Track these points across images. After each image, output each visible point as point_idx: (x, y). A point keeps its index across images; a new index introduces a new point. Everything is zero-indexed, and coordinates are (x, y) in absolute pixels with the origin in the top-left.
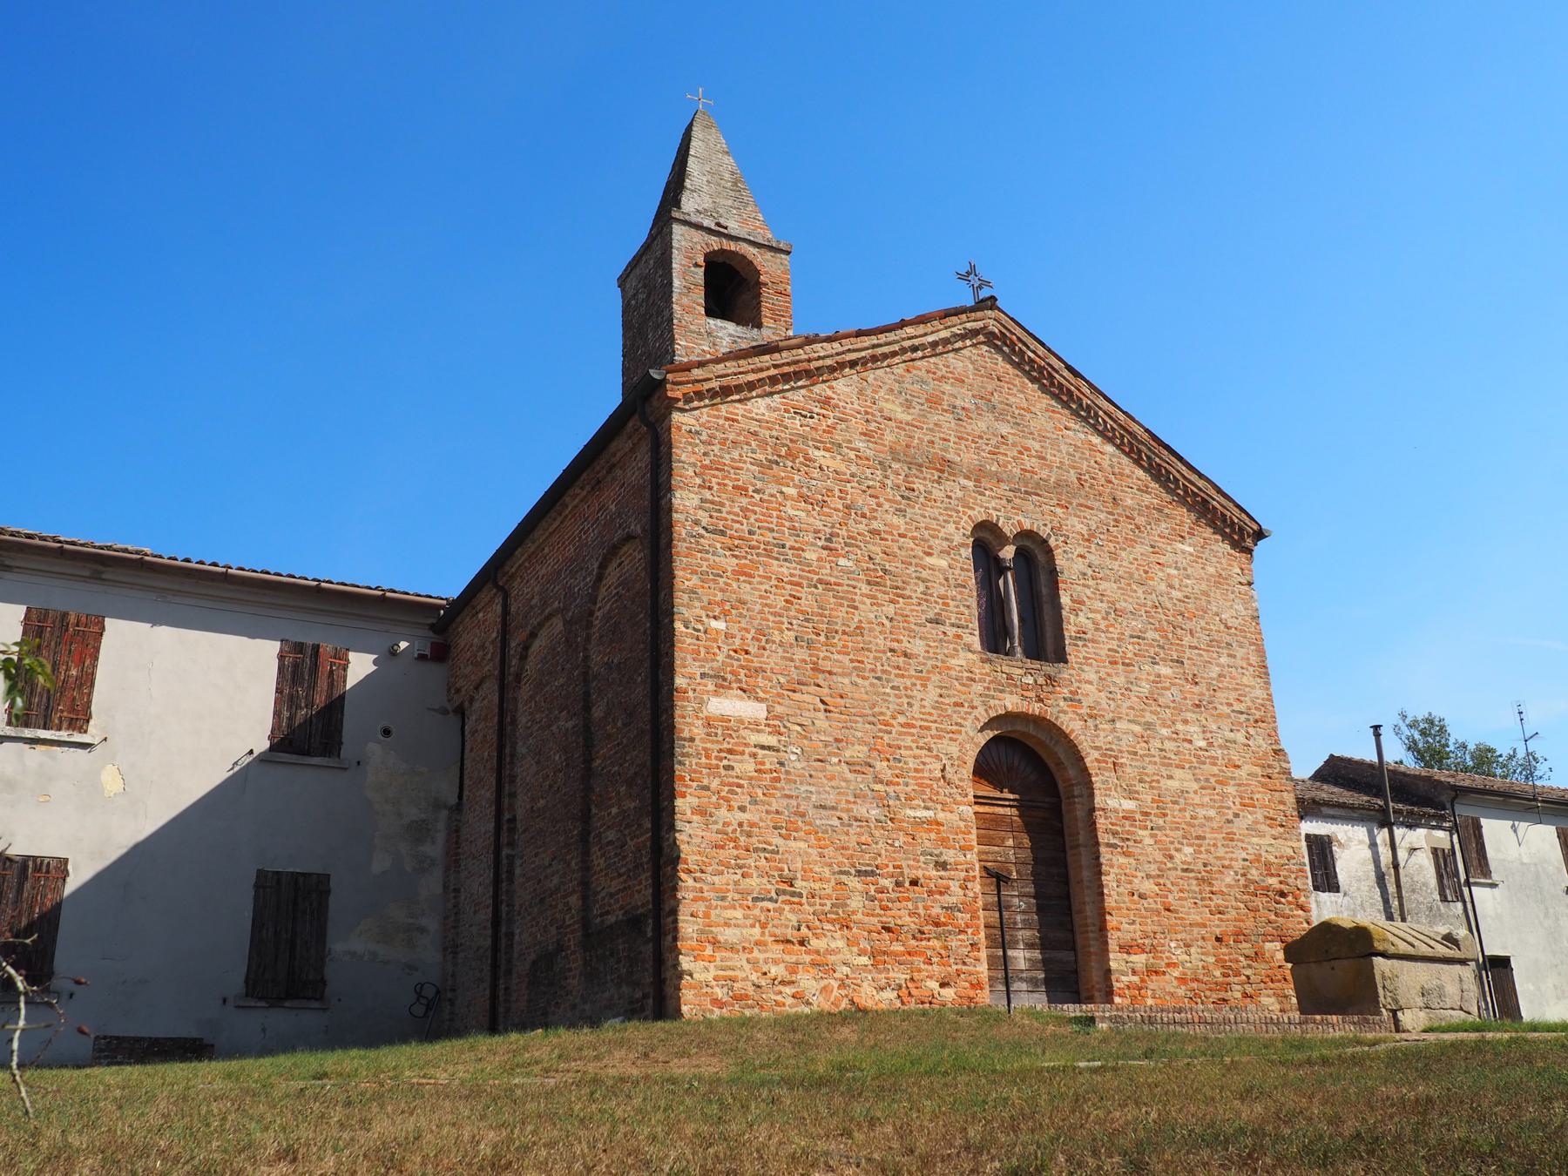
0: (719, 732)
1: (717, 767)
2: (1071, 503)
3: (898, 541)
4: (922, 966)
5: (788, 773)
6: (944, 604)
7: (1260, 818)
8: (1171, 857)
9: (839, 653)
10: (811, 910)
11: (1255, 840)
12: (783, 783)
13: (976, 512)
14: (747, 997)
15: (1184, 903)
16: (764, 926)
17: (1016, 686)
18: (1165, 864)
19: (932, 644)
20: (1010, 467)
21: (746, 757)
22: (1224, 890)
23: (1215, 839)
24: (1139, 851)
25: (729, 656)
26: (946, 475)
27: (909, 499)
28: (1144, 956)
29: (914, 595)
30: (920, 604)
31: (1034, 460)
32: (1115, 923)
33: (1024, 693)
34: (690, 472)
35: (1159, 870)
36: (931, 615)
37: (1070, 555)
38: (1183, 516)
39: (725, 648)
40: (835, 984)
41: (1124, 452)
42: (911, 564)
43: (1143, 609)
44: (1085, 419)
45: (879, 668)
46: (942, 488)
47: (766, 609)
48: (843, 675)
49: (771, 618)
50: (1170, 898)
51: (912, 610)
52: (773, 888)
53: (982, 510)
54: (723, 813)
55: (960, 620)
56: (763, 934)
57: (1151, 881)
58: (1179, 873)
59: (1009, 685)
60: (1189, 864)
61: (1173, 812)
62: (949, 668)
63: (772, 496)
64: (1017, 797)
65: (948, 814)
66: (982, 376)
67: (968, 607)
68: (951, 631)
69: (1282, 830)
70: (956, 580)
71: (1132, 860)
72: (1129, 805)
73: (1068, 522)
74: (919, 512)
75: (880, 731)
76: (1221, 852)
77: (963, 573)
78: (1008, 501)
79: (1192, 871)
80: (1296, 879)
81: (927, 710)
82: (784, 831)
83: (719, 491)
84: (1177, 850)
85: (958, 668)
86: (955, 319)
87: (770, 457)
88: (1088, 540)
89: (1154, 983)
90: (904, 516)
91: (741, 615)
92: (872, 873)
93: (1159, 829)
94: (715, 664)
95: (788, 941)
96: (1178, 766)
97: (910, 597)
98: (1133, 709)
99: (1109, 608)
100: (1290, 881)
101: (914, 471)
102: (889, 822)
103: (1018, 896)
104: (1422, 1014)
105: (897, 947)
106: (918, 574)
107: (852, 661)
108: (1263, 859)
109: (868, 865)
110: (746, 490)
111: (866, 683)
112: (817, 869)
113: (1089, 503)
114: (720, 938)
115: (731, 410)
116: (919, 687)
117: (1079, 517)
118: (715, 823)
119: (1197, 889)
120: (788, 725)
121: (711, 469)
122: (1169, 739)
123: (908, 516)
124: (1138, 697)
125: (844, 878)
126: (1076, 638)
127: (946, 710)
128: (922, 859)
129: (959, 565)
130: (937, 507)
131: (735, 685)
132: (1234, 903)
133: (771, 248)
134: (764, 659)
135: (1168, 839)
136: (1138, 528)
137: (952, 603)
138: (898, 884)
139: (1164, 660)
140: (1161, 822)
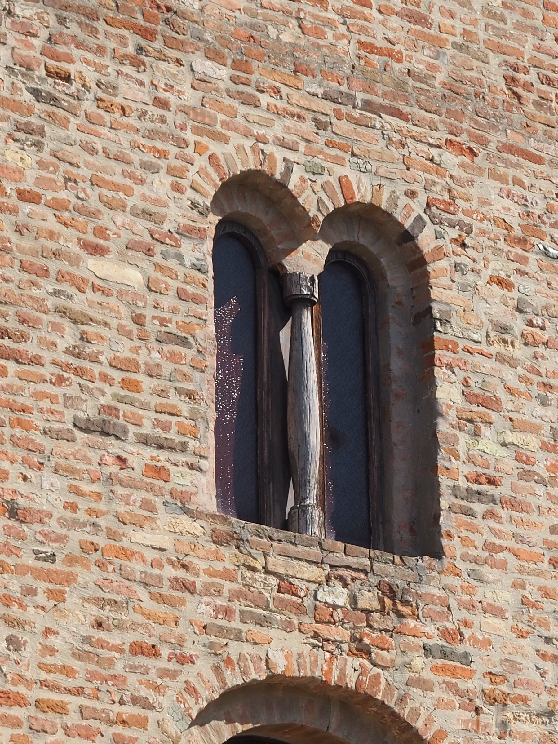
2: (483, 143)
3: (14, 211)
6: (126, 384)
13: (230, 149)
17: (300, 609)
19: (86, 487)
20: (330, 35)
26: (158, 44)
27: (53, 100)
29: (47, 356)
30: (60, 380)
31: (394, 21)
33: (323, 629)
37: (471, 278)
42: (45, 273)
46: (145, 78)
51: (40, 396)
53: (248, 143)
55: (166, 427)
59: (283, 606)
62: (127, 554)
67: (190, 395)
70: (163, 322)
73: (473, 191)
74: (78, 136)
77: (182, 306)
78: (320, 125)
81: (58, 660)
85: (150, 555)
88: (522, 242)
90: (38, 145)
97: (36, 361)
101: (74, 29)
106: (62, 302)
113: (532, 146)
116: (41, 599)
117: (502, 179)
123: (49, 146)
127: (111, 662)
129: (174, 284)
130: (129, 128)
137: (147, 383)
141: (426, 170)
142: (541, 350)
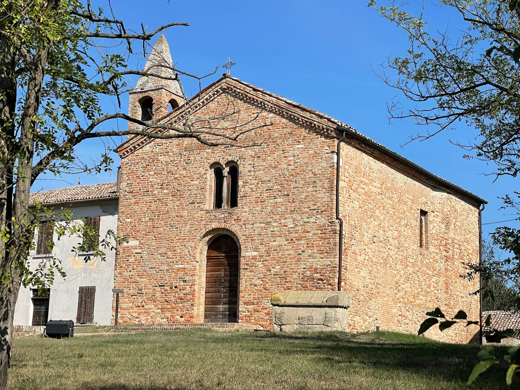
0: (126, 251)
1: (125, 261)
4: (175, 312)
5: (143, 259)
7: (315, 251)
8: (270, 270)
9: (161, 221)
10: (146, 297)
11: (310, 260)
12: (141, 263)
14: (127, 322)
15: (273, 286)
16: (133, 303)
17: (217, 219)
21: (133, 257)
22: (292, 280)
23: (292, 262)
25: (131, 229)
27: (188, 163)
29: (186, 196)
32: (243, 295)
34: (125, 176)
36: (191, 201)
38: (304, 132)
39: (130, 226)
40: (150, 318)
41: (277, 114)
42: (186, 186)
43: (274, 178)
44: (261, 107)
45: (172, 222)
47: (142, 212)
48: (161, 227)
49: (143, 215)
52: (136, 292)
54: (126, 273)
56: (133, 305)
57: (260, 280)
58: (272, 276)
59: (214, 219)
60: (277, 272)
61: (273, 254)
62: (194, 218)
63: (146, 176)
64: (225, 255)
65: (188, 265)
66: (221, 106)
68: (196, 205)
69: (326, 254)
71: (252, 273)
72: (255, 253)
73: (247, 153)
75: (170, 242)
76: (293, 266)
78: (224, 152)
79: (278, 275)
82: (140, 276)
83: (132, 180)
84: (273, 268)
85: (197, 217)
86: (210, 89)
87: (147, 164)
88: (254, 157)
89: (256, 315)
91: (135, 216)
92: (164, 286)
94: (127, 232)
95: (139, 307)
96: (278, 236)
97: (185, 197)
98: (262, 218)
99: (259, 181)
100: (326, 275)
101: (191, 153)
102: (170, 270)
103: (223, 288)
104: (296, 326)
105: (169, 307)
107: (164, 222)
108: (314, 267)
109: (163, 283)
110: (139, 176)
111: (168, 228)
112: (148, 286)
114: (122, 307)
115: (138, 152)
117: (252, 149)
118: (123, 276)
119: (279, 281)
120: (144, 245)
121: (130, 173)
122: (276, 227)
124: (265, 213)
125: (155, 288)
126: (244, 196)
128: (179, 280)
131: (131, 237)
132: (296, 285)
133: (157, 89)
134: (140, 227)
135: (269, 264)
136: (278, 145)
137: (198, 195)
138: (171, 288)
139: (280, 196)
140: (268, 258)
141: (239, 152)
142: (256, 172)
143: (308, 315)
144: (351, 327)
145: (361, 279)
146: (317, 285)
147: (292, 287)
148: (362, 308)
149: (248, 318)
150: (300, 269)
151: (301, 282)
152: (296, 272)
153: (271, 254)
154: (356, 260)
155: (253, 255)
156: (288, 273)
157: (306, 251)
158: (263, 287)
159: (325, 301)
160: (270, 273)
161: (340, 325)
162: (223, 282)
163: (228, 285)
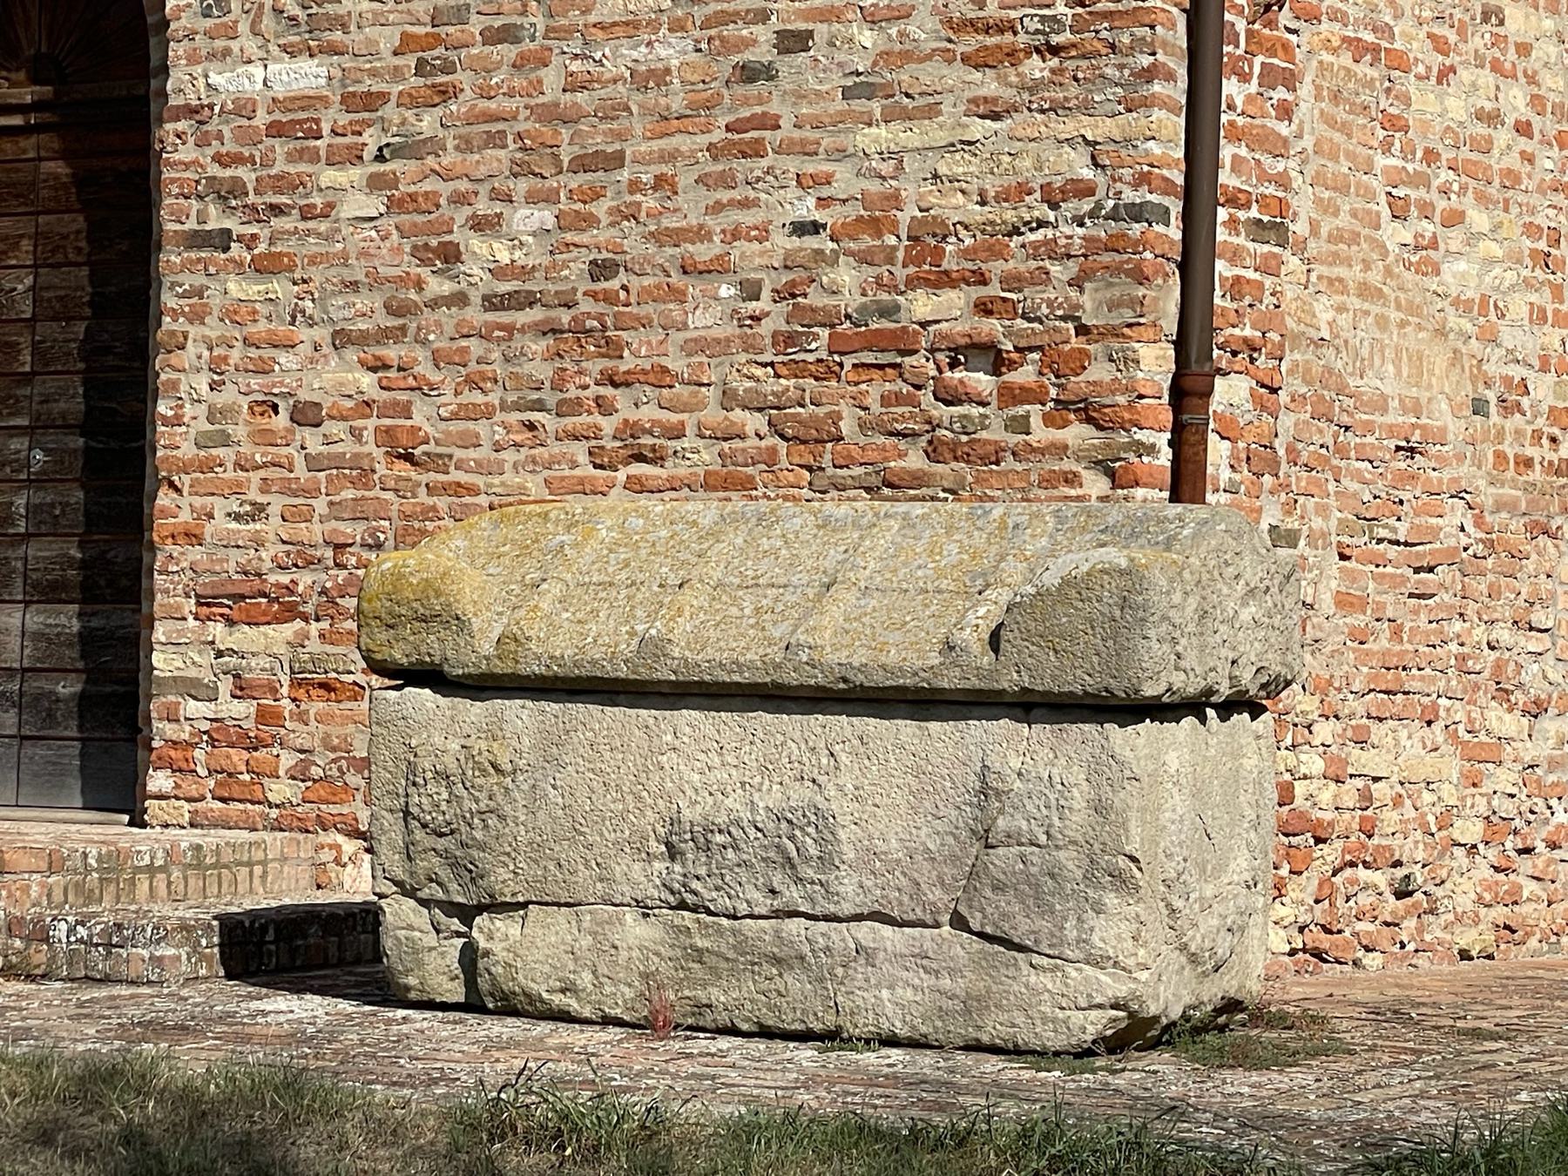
8: (450, 255)
15: (481, 427)
18: (419, 285)
23: (670, 157)
24: (313, 245)
28: (289, 630)
32: (185, 516)
35: (391, 310)
50: (421, 416)
57: (352, 354)
58: (475, 315)
60: (525, 272)
69: (1036, 68)
71: (279, 287)
72: (307, 75)
76: (690, 207)
79: (530, 301)
80: (1077, 283)
84: (479, 225)
93: (411, 149)
100: (1038, 297)
104: (635, 931)
119: (543, 371)
132: (713, 414)
135: (445, 189)
140: (427, 123)
143: (771, 798)
144: (1331, 853)
145: (1441, 332)
146: (942, 412)
147: (677, 433)
148: (1458, 626)
149: (238, 757)
150: (763, 233)
151: (771, 386)
152: (718, 268)
153: (462, 78)
154: (1395, 124)
155: (279, 91)
156: (635, 283)
157: (821, 30)
158: (386, 436)
159: (972, 638)
160: (447, 287)
161: (1157, 930)
162: (28, 378)
163: (73, 403)
